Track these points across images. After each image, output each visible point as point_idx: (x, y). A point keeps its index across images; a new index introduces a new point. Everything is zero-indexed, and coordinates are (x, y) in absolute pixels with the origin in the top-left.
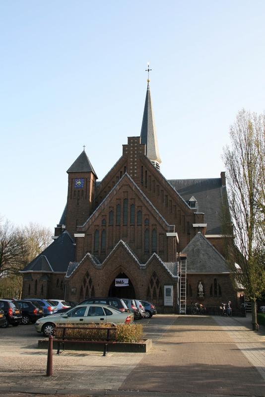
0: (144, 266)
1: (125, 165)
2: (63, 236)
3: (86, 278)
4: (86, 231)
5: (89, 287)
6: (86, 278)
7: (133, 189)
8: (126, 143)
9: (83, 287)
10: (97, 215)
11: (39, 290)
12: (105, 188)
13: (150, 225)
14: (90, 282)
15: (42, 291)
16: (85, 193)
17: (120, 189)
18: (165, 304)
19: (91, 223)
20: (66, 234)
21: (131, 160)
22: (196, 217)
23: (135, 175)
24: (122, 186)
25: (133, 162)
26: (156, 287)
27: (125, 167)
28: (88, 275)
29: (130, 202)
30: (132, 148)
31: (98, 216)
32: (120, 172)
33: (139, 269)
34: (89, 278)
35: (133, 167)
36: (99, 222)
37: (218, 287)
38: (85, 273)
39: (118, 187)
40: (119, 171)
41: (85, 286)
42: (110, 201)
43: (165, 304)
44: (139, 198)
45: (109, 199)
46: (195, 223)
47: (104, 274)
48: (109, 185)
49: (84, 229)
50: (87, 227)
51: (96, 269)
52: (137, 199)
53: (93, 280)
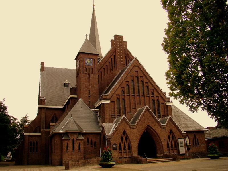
0: (164, 125)
1: (114, 54)
3: (123, 136)
4: (110, 99)
5: (126, 143)
6: (123, 136)
7: (142, 69)
8: (113, 39)
9: (121, 143)
10: (118, 86)
11: (76, 148)
13: (155, 97)
14: (127, 138)
15: (79, 149)
16: (94, 70)
17: (132, 68)
18: (180, 153)
19: (113, 93)
21: (119, 51)
23: (122, 62)
24: (133, 67)
25: (120, 53)
27: (114, 56)
28: (124, 133)
29: (140, 79)
30: (118, 43)
32: (110, 59)
33: (161, 127)
35: (120, 57)
36: (119, 92)
37: (196, 140)
38: (123, 131)
41: (122, 142)
43: (180, 153)
44: (146, 77)
45: (126, 75)
47: (137, 132)
48: (103, 67)
49: (108, 96)
50: (111, 95)
51: (131, 128)
52: (144, 77)
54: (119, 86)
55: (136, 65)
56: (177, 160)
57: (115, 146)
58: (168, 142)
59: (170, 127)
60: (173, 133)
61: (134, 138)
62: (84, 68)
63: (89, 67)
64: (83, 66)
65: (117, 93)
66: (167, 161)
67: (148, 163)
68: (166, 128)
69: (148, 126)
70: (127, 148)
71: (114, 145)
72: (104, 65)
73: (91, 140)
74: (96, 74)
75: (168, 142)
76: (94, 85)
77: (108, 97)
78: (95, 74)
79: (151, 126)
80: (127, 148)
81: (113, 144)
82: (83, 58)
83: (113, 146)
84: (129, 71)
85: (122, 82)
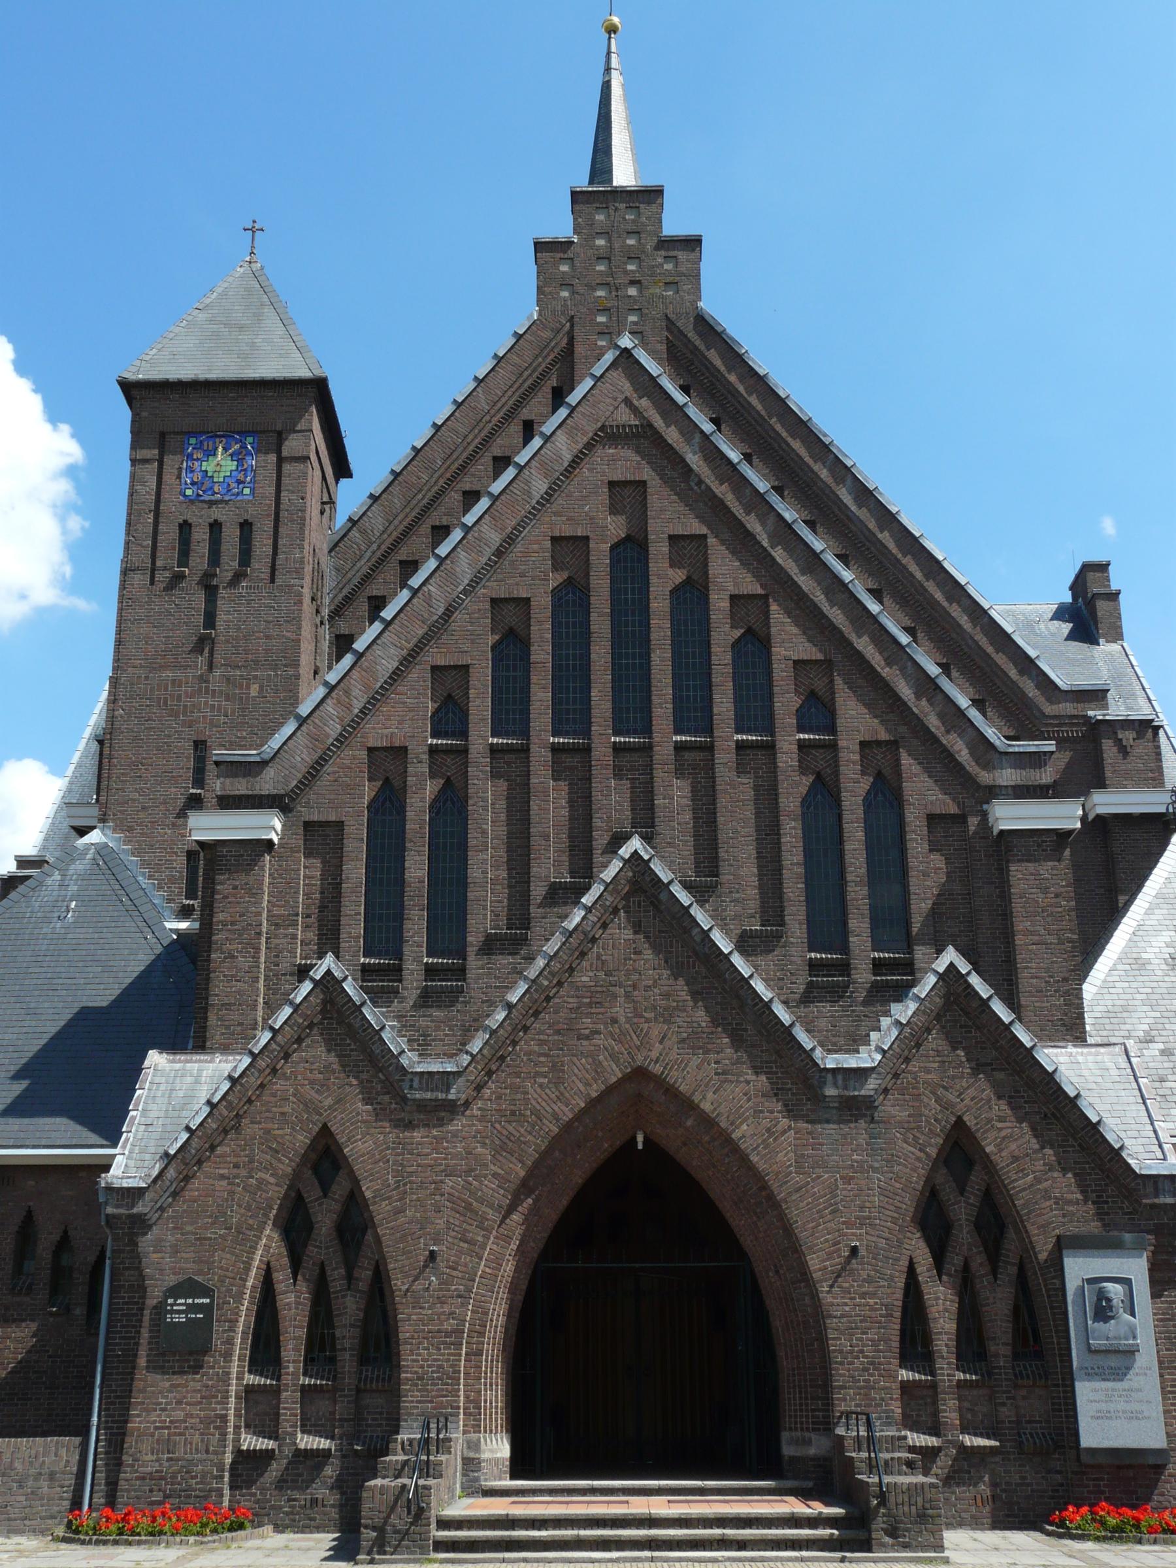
0: (861, 1074)
2: (79, 866)
3: (312, 1193)
5: (336, 1275)
6: (312, 1193)
8: (561, 226)
10: (387, 663)
12: (406, 533)
17: (576, 462)
18: (1088, 1439)
19: (333, 730)
20: (101, 849)
22: (1108, 748)
26: (979, 1262)
31: (396, 675)
34: (340, 1189)
38: (302, 1140)
39: (565, 448)
40: (510, 415)
42: (499, 553)
43: (1088, 1439)
45: (495, 538)
46: (1101, 784)
50: (302, 757)
53: (381, 1211)
54: (410, 659)
55: (624, 417)
56: (893, 1532)
57: (192, 1308)
58: (913, 1289)
59: (951, 1097)
60: (988, 1164)
61: (441, 1223)
62: (169, 533)
63: (216, 513)
64: (157, 513)
65: (377, 733)
66: (742, 1545)
67: (440, 1546)
68: (890, 1108)
69: (640, 1074)
70: (347, 1334)
71: (175, 1291)
72: (441, 493)
73: (65, 1232)
74: (278, 582)
75: (913, 1289)
76: (254, 690)
77: (268, 782)
78: (273, 581)
79: (674, 1076)
80: (347, 1334)
81: (171, 1280)
82: (163, 435)
83: (160, 1310)
84: (540, 486)
85: (449, 613)
